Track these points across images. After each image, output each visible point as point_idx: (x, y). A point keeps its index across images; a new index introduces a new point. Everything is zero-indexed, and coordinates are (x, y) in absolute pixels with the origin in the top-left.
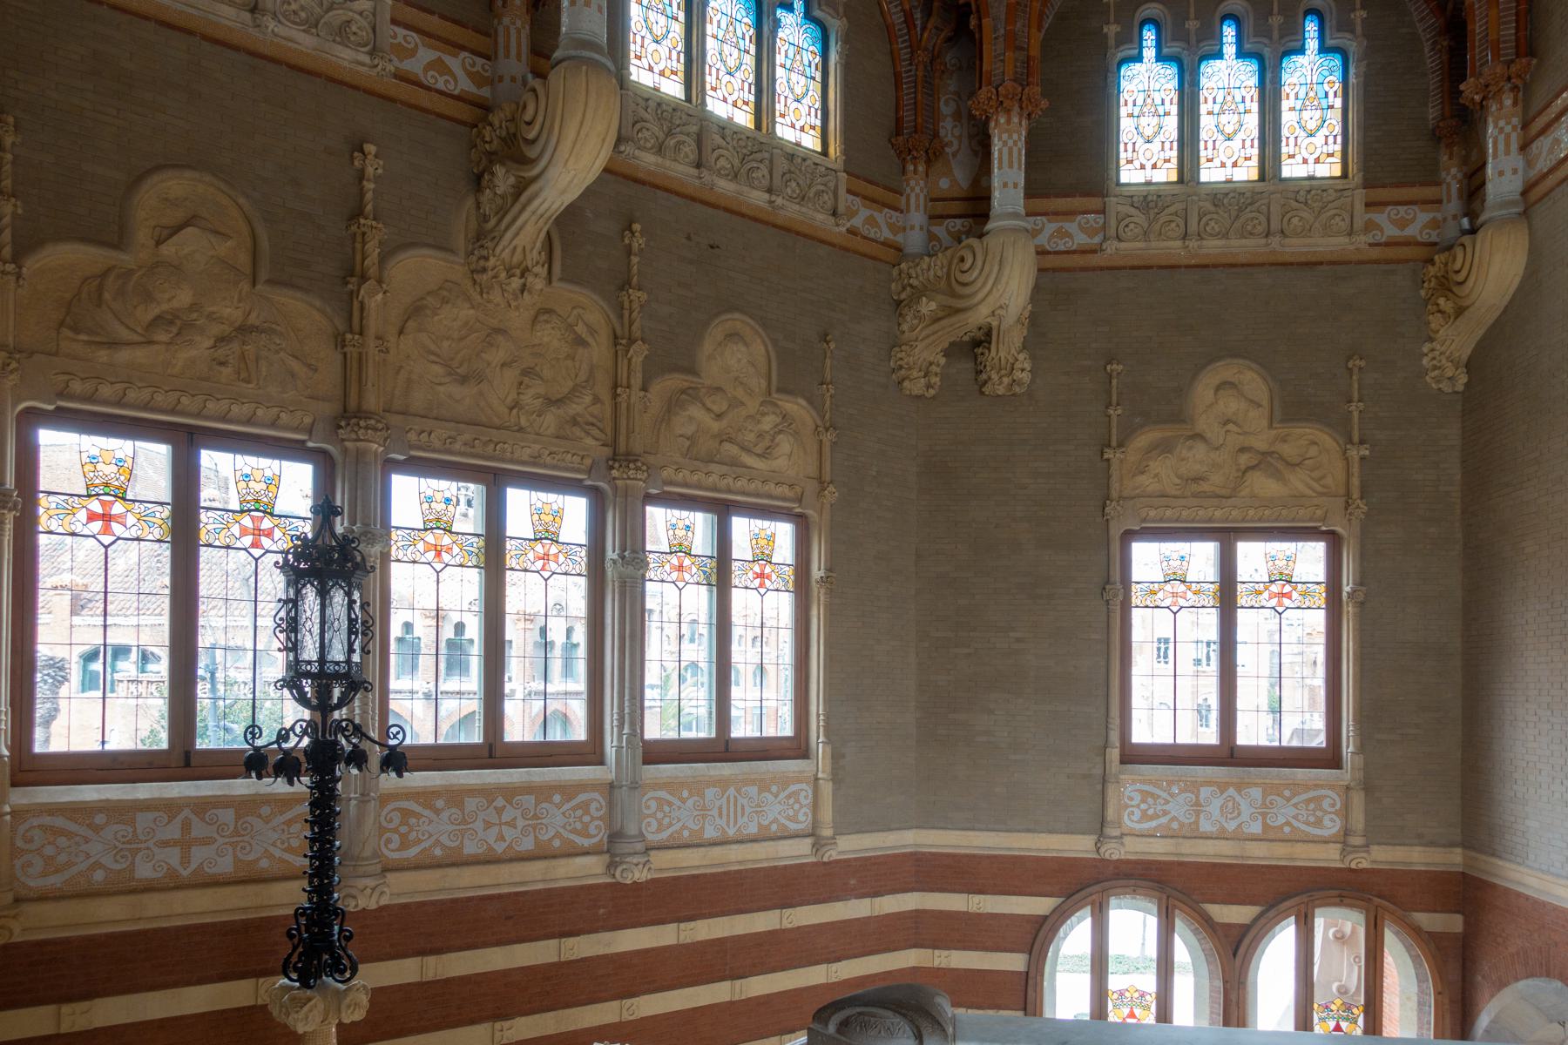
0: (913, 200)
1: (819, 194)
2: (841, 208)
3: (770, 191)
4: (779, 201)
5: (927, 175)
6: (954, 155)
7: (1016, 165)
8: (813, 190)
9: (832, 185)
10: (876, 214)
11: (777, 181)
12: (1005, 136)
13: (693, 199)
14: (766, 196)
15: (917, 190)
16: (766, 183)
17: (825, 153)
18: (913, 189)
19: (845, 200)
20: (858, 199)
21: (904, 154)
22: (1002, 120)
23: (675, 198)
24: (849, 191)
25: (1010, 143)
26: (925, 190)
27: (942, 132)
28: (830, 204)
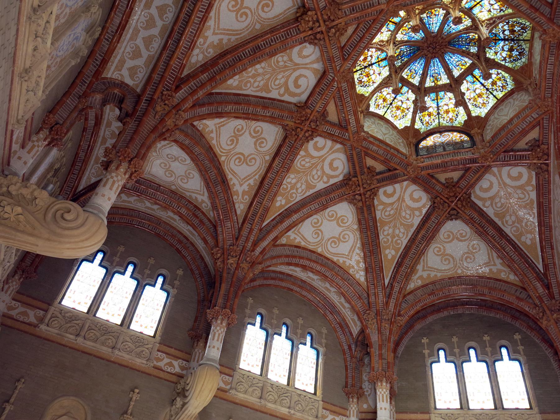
0: (352, 412)
1: (311, 409)
2: (320, 415)
3: (289, 408)
4: (292, 412)
5: (358, 403)
6: (369, 395)
7: (385, 401)
8: (308, 408)
9: (316, 406)
10: (336, 418)
11: (292, 405)
12: (381, 390)
13: (257, 410)
14: (288, 410)
15: (354, 408)
16: (288, 405)
17: (315, 394)
18: (352, 408)
19: (322, 412)
20: (328, 412)
21: (348, 394)
22: (379, 384)
23: (249, 409)
24: (324, 408)
25: (383, 393)
26: (357, 409)
27: (363, 387)
28: (315, 414)
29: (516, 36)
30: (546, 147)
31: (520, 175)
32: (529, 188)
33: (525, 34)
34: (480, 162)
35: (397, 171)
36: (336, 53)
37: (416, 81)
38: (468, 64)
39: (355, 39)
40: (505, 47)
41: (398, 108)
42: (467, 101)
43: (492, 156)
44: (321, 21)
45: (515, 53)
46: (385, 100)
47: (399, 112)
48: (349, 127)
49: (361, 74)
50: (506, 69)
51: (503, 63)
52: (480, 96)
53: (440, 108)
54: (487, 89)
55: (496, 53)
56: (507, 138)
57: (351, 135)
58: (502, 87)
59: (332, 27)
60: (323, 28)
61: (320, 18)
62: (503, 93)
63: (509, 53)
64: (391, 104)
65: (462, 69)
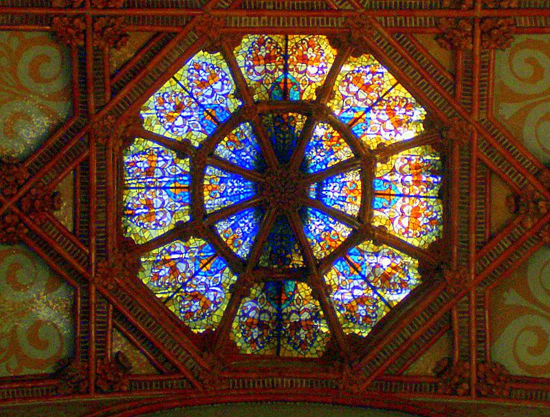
29: (286, 332)
30: (125, 388)
31: (43, 345)
32: (14, 365)
33: (289, 347)
34: (100, 265)
35: (108, 94)
36: (412, 23)
37: (223, 150)
38: (235, 250)
39: (422, 58)
40: (267, 316)
41: (179, 108)
42: (167, 247)
43: (111, 287)
44: (495, 13)
45: (256, 332)
46: (204, 84)
47: (170, 107)
48: (245, 13)
49: (276, 48)
50: (229, 316)
51: (239, 312)
52: (174, 270)
53: (158, 192)
54: (184, 285)
55: (255, 300)
56: (144, 316)
57: (224, 13)
58: (189, 311)
59: (473, 27)
60: (479, 13)
61: (503, 13)
62: (177, 313)
63: (255, 322)
64: (191, 95)
65: (227, 238)
